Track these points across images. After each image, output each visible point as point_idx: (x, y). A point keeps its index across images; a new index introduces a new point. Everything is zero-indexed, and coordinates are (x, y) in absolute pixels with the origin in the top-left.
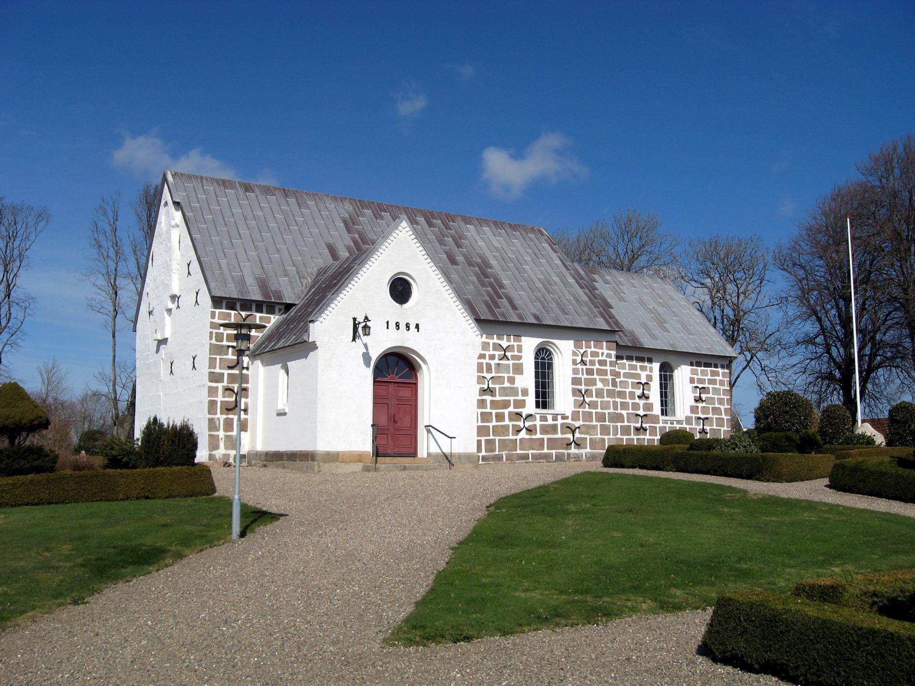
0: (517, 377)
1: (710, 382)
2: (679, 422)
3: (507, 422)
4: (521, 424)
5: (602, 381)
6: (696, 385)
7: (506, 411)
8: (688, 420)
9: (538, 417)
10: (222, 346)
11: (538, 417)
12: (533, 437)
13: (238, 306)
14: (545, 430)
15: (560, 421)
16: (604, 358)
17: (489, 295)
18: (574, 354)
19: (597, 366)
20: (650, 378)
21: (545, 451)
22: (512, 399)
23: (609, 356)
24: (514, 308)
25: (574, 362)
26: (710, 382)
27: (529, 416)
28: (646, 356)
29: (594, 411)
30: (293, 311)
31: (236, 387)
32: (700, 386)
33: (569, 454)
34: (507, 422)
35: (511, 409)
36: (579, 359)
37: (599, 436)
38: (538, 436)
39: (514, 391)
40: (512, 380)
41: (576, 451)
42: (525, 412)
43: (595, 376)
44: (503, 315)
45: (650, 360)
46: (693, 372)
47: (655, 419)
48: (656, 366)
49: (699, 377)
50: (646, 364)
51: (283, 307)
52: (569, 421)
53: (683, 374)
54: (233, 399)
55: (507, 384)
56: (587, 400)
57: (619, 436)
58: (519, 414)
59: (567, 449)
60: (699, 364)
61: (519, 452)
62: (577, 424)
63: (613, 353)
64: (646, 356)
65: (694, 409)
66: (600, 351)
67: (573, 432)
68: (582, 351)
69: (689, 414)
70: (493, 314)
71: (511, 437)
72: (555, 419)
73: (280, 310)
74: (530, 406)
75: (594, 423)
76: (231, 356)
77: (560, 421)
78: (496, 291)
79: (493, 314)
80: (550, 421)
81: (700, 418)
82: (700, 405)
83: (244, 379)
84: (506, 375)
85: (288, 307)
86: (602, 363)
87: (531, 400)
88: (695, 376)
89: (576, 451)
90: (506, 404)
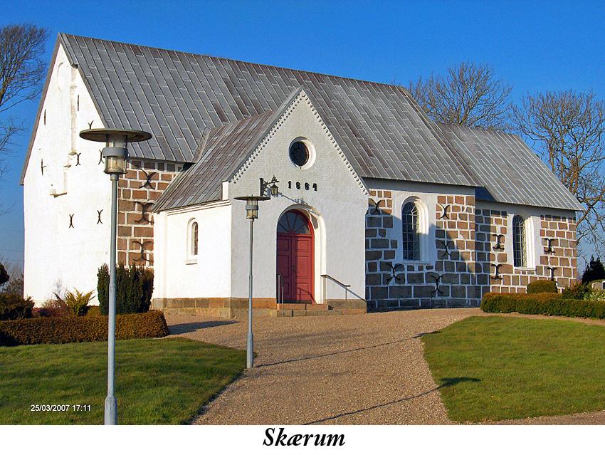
0: (387, 229)
1: (559, 234)
2: (530, 272)
3: (378, 271)
4: (391, 273)
5: (462, 233)
6: (546, 237)
7: (378, 262)
8: (538, 270)
9: (406, 267)
10: (129, 202)
11: (406, 267)
12: (402, 285)
13: (143, 164)
14: (412, 279)
15: (425, 271)
16: (464, 212)
17: (362, 154)
18: (438, 208)
19: (458, 219)
20: (504, 230)
21: (413, 298)
22: (383, 250)
23: (468, 210)
24: (385, 166)
25: (438, 215)
26: (559, 234)
27: (399, 267)
28: (501, 209)
29: (455, 261)
30: (192, 171)
31: (142, 239)
32: (550, 238)
33: (433, 301)
34: (378, 271)
35: (382, 259)
36: (442, 213)
37: (460, 284)
38: (406, 284)
39: (384, 243)
40: (383, 233)
41: (440, 298)
42: (394, 262)
43: (456, 229)
44: (375, 172)
45: (504, 214)
46: (544, 225)
47: (509, 269)
48: (510, 217)
49: (549, 229)
50: (501, 217)
51: (182, 166)
52: (434, 270)
53: (531, 226)
54: (139, 251)
55: (378, 237)
56: (449, 251)
57: (477, 285)
58: (390, 265)
59: (431, 297)
60: (548, 217)
61: (389, 299)
62: (440, 274)
63: (473, 208)
64: (501, 209)
65: (543, 260)
66: (461, 206)
67: (437, 281)
68: (445, 206)
69: (540, 265)
70: (368, 172)
71: (382, 285)
72: (421, 268)
73: (179, 169)
74: (399, 258)
75: (456, 273)
76: (137, 211)
77: (425, 271)
78: (368, 151)
79: (368, 172)
80: (416, 271)
81: (549, 268)
82: (549, 256)
83: (150, 233)
84: (378, 228)
85: (187, 166)
86: (463, 217)
87: (399, 251)
88: (545, 229)
89: (440, 298)
90: (378, 255)
